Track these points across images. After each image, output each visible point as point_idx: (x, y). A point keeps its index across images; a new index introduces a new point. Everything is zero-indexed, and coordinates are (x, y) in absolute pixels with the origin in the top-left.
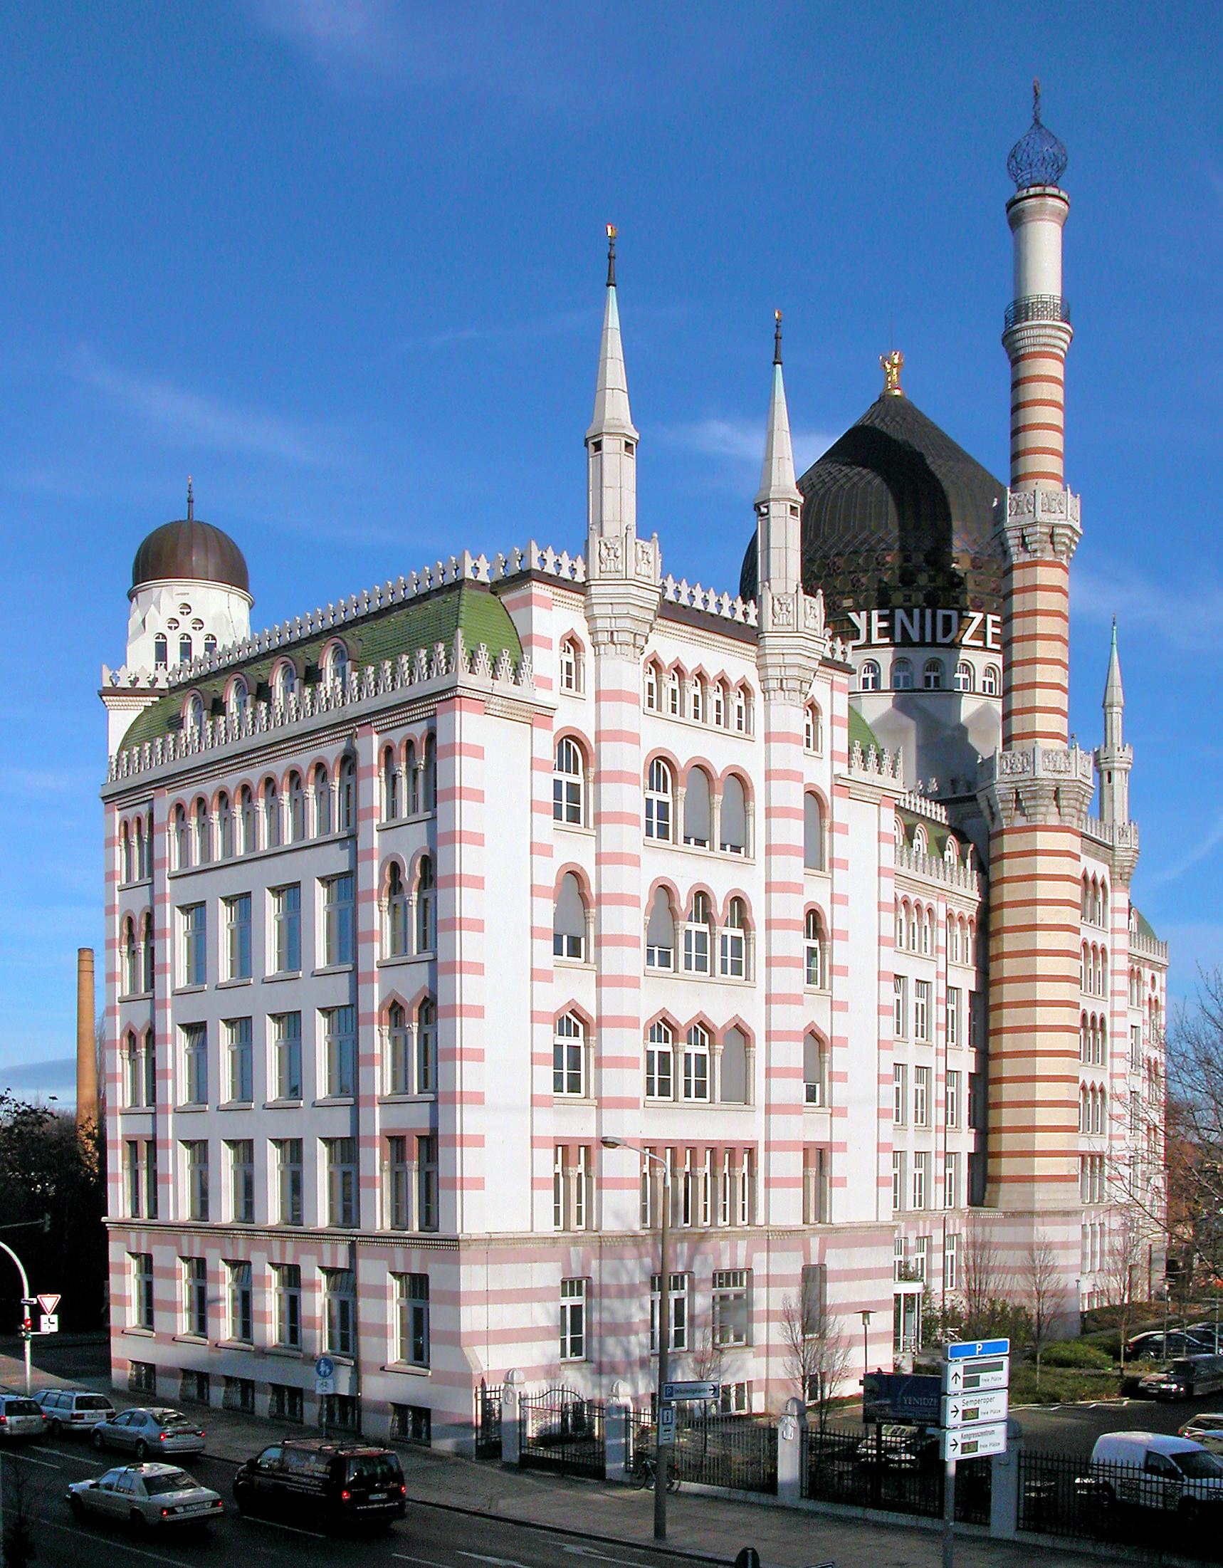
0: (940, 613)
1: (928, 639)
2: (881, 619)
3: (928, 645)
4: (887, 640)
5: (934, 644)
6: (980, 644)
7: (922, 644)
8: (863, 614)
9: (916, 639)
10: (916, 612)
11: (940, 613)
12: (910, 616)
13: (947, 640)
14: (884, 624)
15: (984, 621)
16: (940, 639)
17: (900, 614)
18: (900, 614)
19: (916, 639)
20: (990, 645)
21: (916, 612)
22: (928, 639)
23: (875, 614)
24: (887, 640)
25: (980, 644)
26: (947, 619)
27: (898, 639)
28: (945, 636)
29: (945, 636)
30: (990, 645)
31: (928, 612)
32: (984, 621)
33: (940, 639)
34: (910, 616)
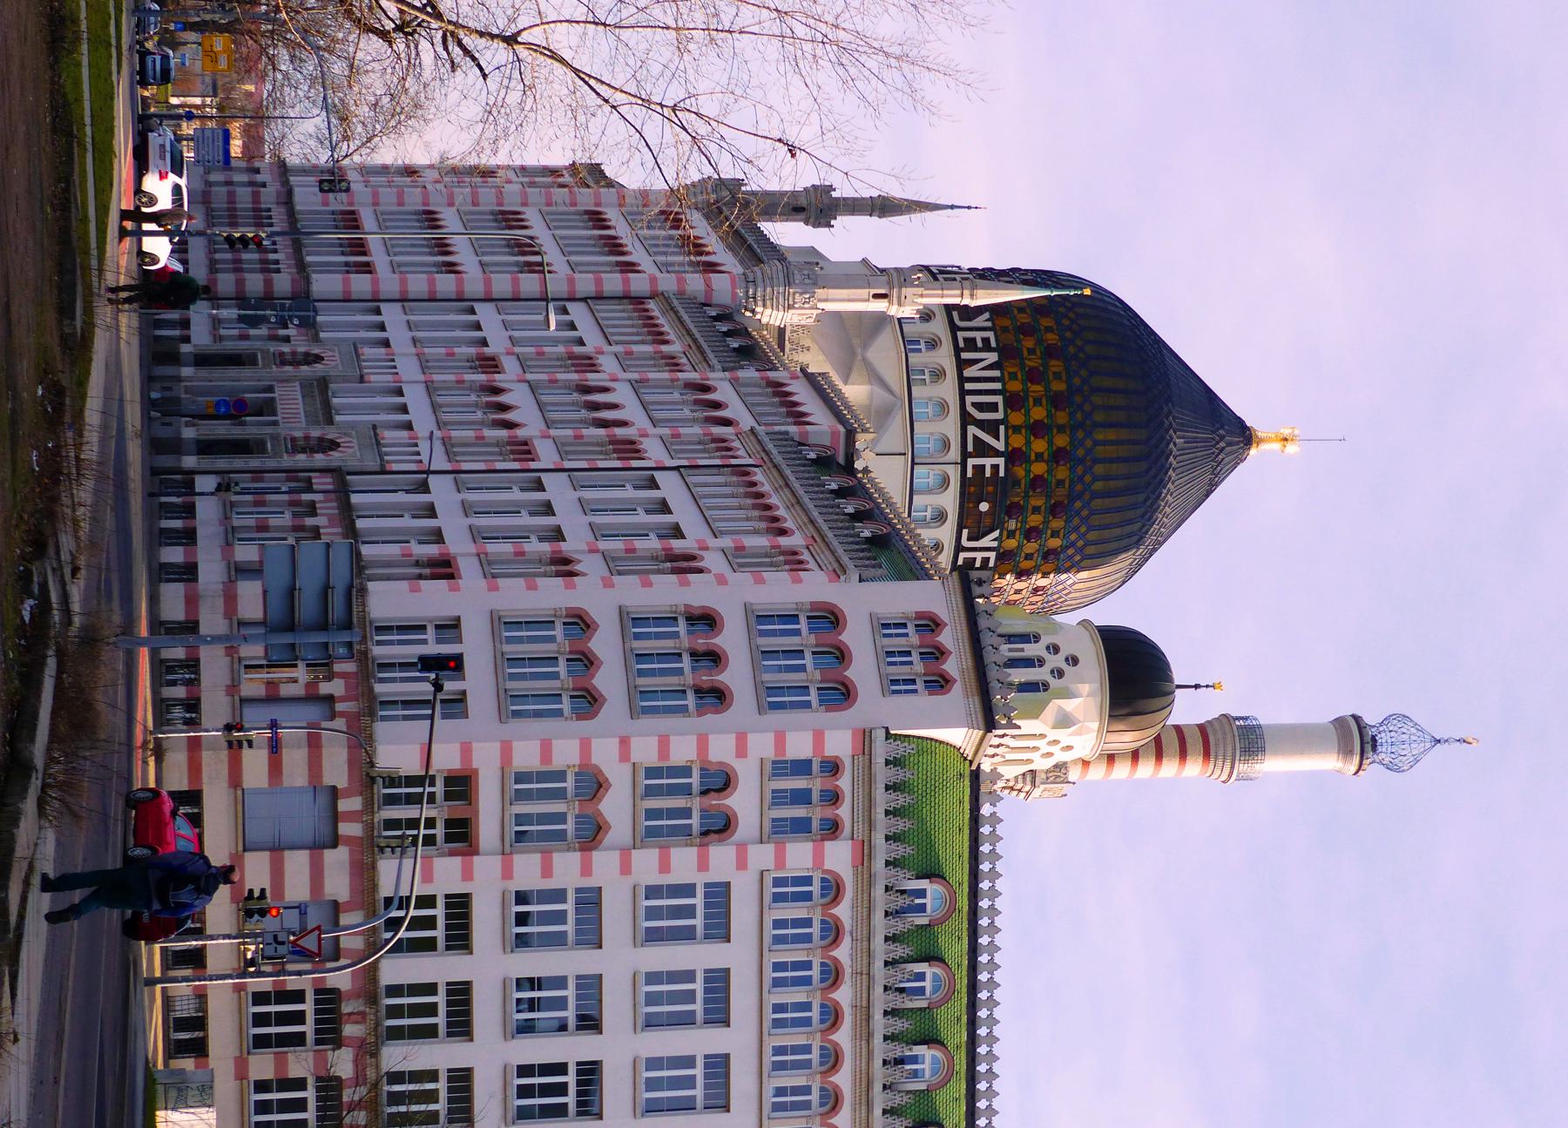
0: (999, 399)
1: (968, 386)
2: (986, 341)
4: (961, 344)
5: (963, 393)
6: (970, 448)
7: (962, 380)
8: (989, 324)
9: (967, 373)
10: (996, 373)
11: (999, 399)
12: (990, 367)
13: (970, 409)
14: (980, 344)
15: (997, 454)
16: (969, 399)
17: (992, 357)
18: (992, 357)
19: (967, 373)
20: (971, 462)
21: (996, 373)
22: (968, 386)
23: (990, 334)
24: (961, 344)
25: (970, 448)
26: (993, 407)
27: (964, 355)
29: (974, 404)
30: (971, 462)
31: (998, 386)
33: (969, 399)
34: (990, 367)
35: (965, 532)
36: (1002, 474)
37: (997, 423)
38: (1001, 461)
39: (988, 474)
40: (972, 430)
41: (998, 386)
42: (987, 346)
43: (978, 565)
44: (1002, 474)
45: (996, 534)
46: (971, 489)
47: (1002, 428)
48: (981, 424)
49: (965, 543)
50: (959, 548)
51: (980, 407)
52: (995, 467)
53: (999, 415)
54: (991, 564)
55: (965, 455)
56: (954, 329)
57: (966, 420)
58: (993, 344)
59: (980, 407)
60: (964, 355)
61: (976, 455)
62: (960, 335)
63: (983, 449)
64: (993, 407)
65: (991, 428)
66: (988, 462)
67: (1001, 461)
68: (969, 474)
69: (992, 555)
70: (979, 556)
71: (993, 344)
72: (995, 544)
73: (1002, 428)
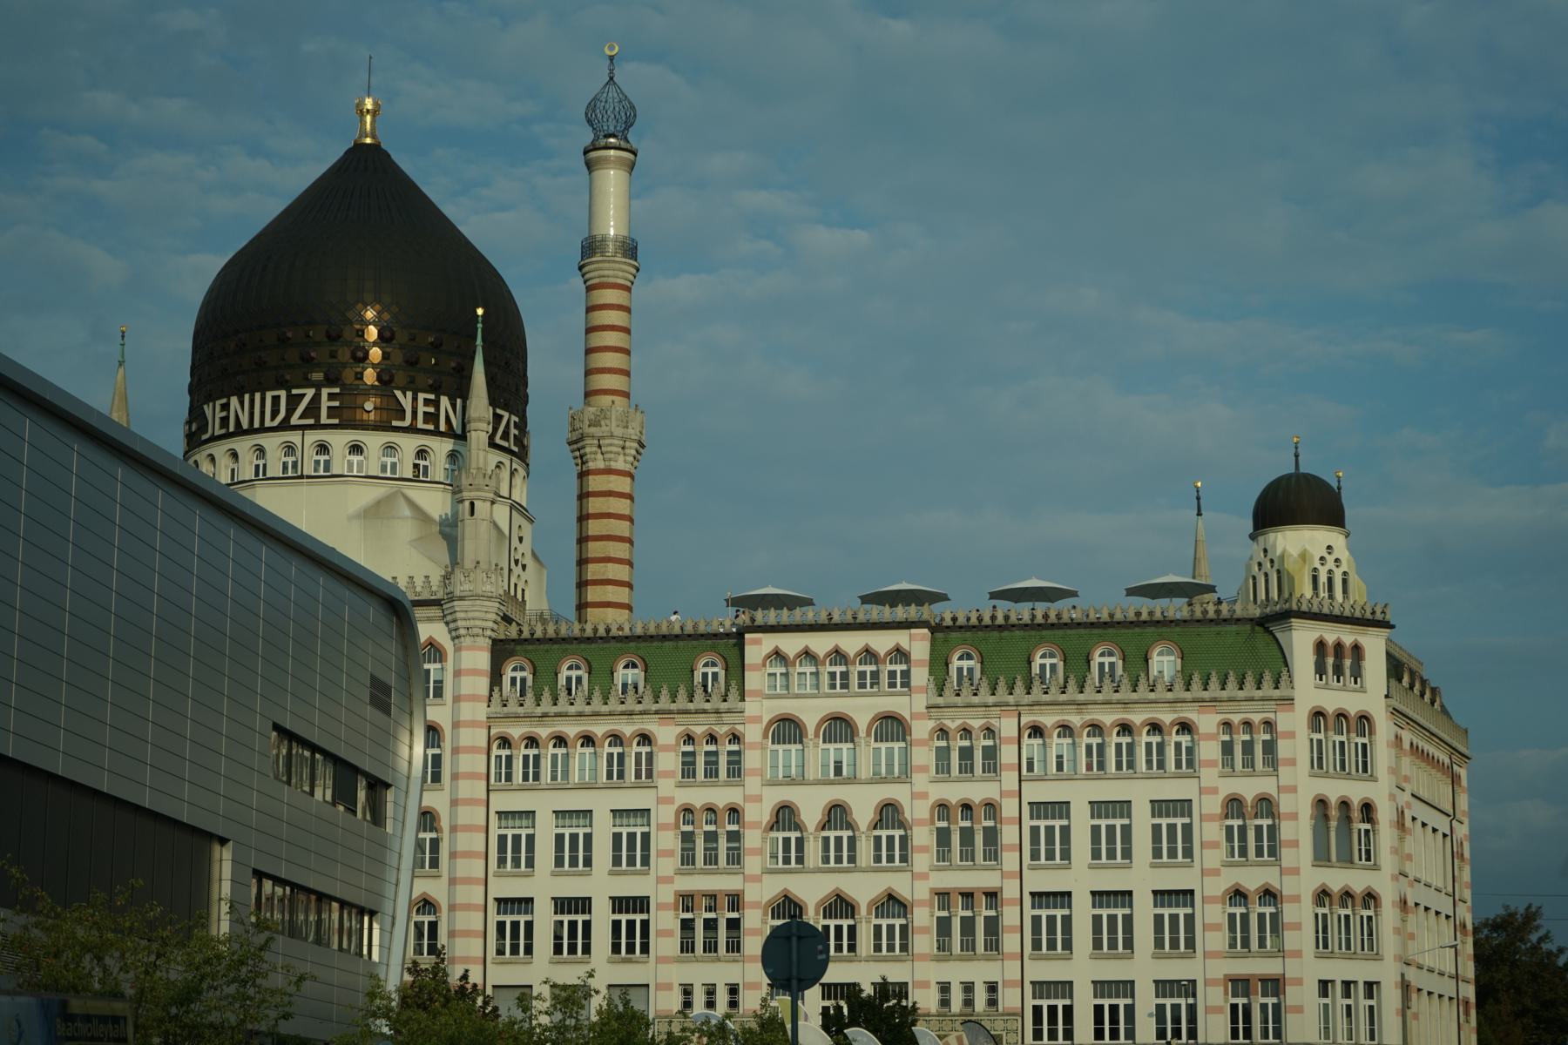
0: (269, 395)
1: (257, 425)
3: (257, 431)
5: (263, 429)
6: (311, 421)
7: (251, 431)
10: (247, 397)
11: (269, 395)
12: (242, 403)
14: (224, 414)
15: (316, 399)
16: (268, 423)
17: (234, 401)
18: (234, 401)
19: (245, 425)
20: (324, 420)
21: (247, 397)
22: (257, 425)
23: (218, 403)
24: (223, 431)
25: (311, 421)
26: (276, 399)
27: (232, 429)
28: (273, 418)
29: (273, 418)
30: (324, 420)
31: (258, 396)
32: (316, 399)
33: (268, 423)
34: (242, 403)
35: (395, 423)
36: (337, 390)
37: (289, 396)
38: (325, 392)
39: (336, 404)
40: (294, 420)
41: (258, 396)
42: (226, 407)
43: (431, 410)
44: (337, 390)
45: (398, 394)
46: (347, 419)
47: (294, 392)
48: (290, 412)
49: (407, 423)
50: (412, 429)
51: (275, 413)
52: (331, 397)
53: (283, 394)
54: (432, 397)
55: (318, 426)
56: (214, 439)
57: (285, 426)
58: (224, 401)
59: (275, 413)
60: (232, 429)
61: (318, 418)
62: (218, 432)
63: (313, 409)
64: (276, 399)
65: (293, 401)
66: (325, 404)
67: (325, 392)
68: (336, 421)
69: (421, 396)
70: (421, 409)
71: (224, 401)
72: (409, 394)
73: (294, 392)
